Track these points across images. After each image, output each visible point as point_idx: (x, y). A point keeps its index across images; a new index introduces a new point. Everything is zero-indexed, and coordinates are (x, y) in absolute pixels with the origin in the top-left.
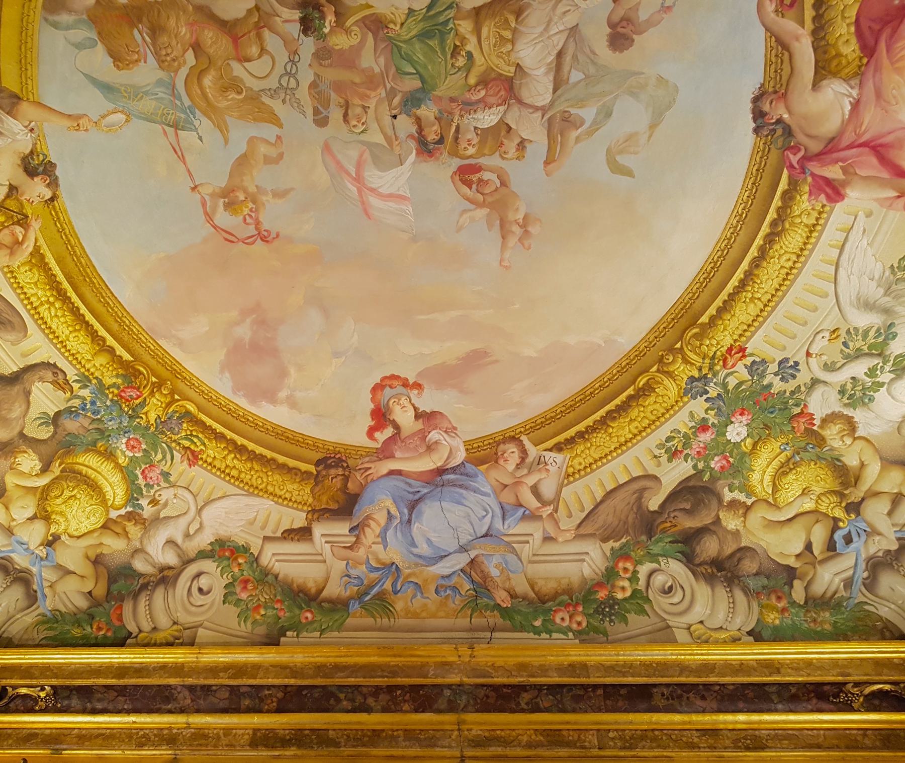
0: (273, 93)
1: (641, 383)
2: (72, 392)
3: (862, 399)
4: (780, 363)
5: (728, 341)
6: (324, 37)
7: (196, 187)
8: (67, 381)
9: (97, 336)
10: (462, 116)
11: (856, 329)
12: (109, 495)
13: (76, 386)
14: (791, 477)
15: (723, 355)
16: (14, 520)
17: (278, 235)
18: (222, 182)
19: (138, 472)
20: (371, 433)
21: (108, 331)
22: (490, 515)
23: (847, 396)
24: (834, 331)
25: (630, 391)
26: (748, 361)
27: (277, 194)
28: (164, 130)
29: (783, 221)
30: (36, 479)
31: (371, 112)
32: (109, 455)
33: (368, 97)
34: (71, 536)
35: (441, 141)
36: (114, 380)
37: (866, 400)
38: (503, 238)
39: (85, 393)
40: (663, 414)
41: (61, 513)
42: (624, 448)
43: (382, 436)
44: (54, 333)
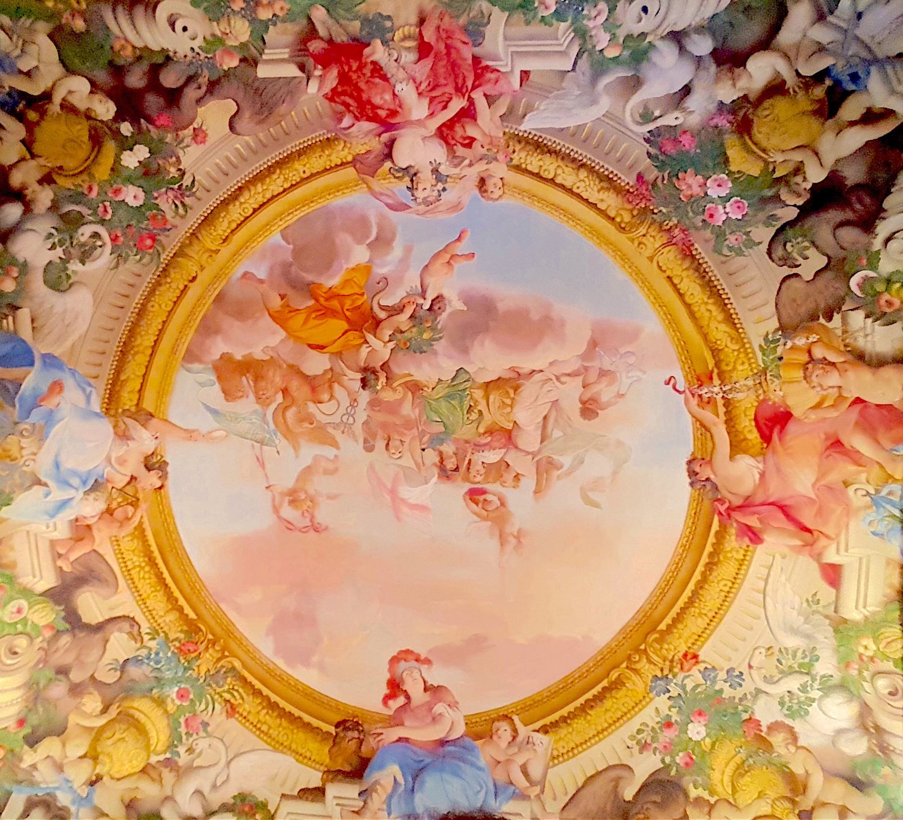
1: (613, 679)
2: (142, 642)
5: (683, 648)
12: (153, 741)
13: (146, 637)
14: (747, 779)
16: (66, 757)
19: (182, 720)
20: (387, 698)
22: (483, 792)
25: (605, 683)
29: (718, 554)
32: (160, 702)
34: (112, 778)
40: (633, 708)
41: (109, 755)
42: (601, 736)
43: (395, 704)
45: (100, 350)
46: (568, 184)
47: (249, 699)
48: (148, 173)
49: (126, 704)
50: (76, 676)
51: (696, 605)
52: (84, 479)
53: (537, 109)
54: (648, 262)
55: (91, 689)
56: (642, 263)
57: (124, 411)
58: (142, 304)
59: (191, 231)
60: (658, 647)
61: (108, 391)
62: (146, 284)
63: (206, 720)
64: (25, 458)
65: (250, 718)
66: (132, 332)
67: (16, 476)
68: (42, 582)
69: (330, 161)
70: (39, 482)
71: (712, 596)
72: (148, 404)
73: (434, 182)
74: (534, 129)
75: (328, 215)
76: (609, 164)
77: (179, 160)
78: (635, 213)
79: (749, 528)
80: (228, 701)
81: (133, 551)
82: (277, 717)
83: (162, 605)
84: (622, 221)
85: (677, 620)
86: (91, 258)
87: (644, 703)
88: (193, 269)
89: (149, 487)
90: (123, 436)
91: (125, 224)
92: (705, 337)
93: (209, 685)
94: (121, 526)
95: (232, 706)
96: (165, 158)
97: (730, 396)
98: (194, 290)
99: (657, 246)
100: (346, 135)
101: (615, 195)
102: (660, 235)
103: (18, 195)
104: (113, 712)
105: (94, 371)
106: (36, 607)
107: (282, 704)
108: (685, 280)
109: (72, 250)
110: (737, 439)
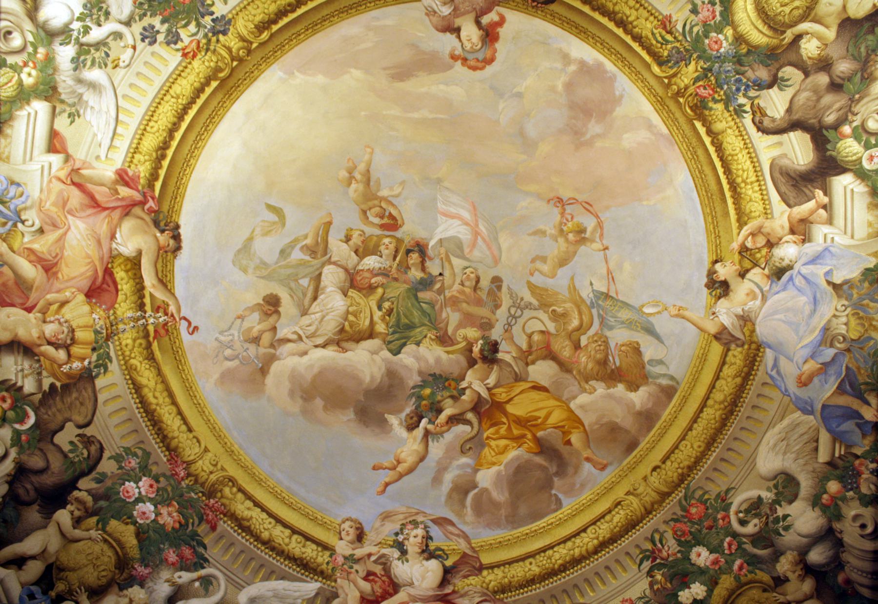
0: (529, 306)
1: (265, 33)
2: (752, 104)
3: (93, 7)
4: (155, 41)
5: (196, 63)
6: (483, 338)
7: (604, 249)
8: (753, 114)
9: (716, 147)
10: (391, 267)
11: (100, 67)
13: (747, 108)
15: (200, 51)
17: (549, 201)
18: (583, 249)
21: (706, 150)
23: (103, 10)
24: (116, 66)
25: (275, 28)
26: (180, 45)
27: (543, 233)
28: (617, 294)
29: (157, 158)
30: (810, 30)
31: (458, 281)
32: (739, 39)
33: (458, 292)
35: (408, 252)
36: (714, 106)
37: (89, 5)
38: (368, 171)
39: (742, 100)
44: (750, 157)
45: (756, 411)
46: (280, 528)
47: (646, 33)
48: (682, 574)
49: (775, 41)
50: (823, 79)
51: (180, 107)
52: (791, 283)
53: (303, 600)
54: (210, 447)
55: (809, 62)
56: (215, 447)
57: (742, 345)
58: (709, 450)
59: (651, 516)
60: (220, 64)
61: (755, 368)
62: (703, 470)
63: (693, 17)
64: (846, 313)
65: (645, 14)
66: (724, 423)
67: (855, 296)
68: (845, 183)
69: (503, 572)
70: (836, 287)
71: (166, 115)
72: (717, 349)
73: (406, 542)
74: (307, 582)
75: (514, 521)
76: (242, 543)
77: (651, 585)
78: (219, 495)
79: (127, 184)
80: (668, 32)
81: (751, 200)
82: (618, 13)
83: (729, 139)
84: (231, 488)
85: (199, 91)
86: (752, 501)
87: (238, 9)
88: (654, 479)
89: (728, 264)
90: (746, 320)
91: (714, 530)
92: (159, 373)
93: (687, 51)
94: (761, 228)
95: (665, 28)
96: (664, 588)
97: (139, 313)
98: (655, 457)
99: (200, 462)
100: (485, 594)
101: (238, 512)
102: (197, 472)
103: (808, 570)
104: (789, 35)
105: (767, 391)
106: (854, 158)
107: (611, 25)
108: (176, 428)
109: (768, 512)
110: (134, 271)
